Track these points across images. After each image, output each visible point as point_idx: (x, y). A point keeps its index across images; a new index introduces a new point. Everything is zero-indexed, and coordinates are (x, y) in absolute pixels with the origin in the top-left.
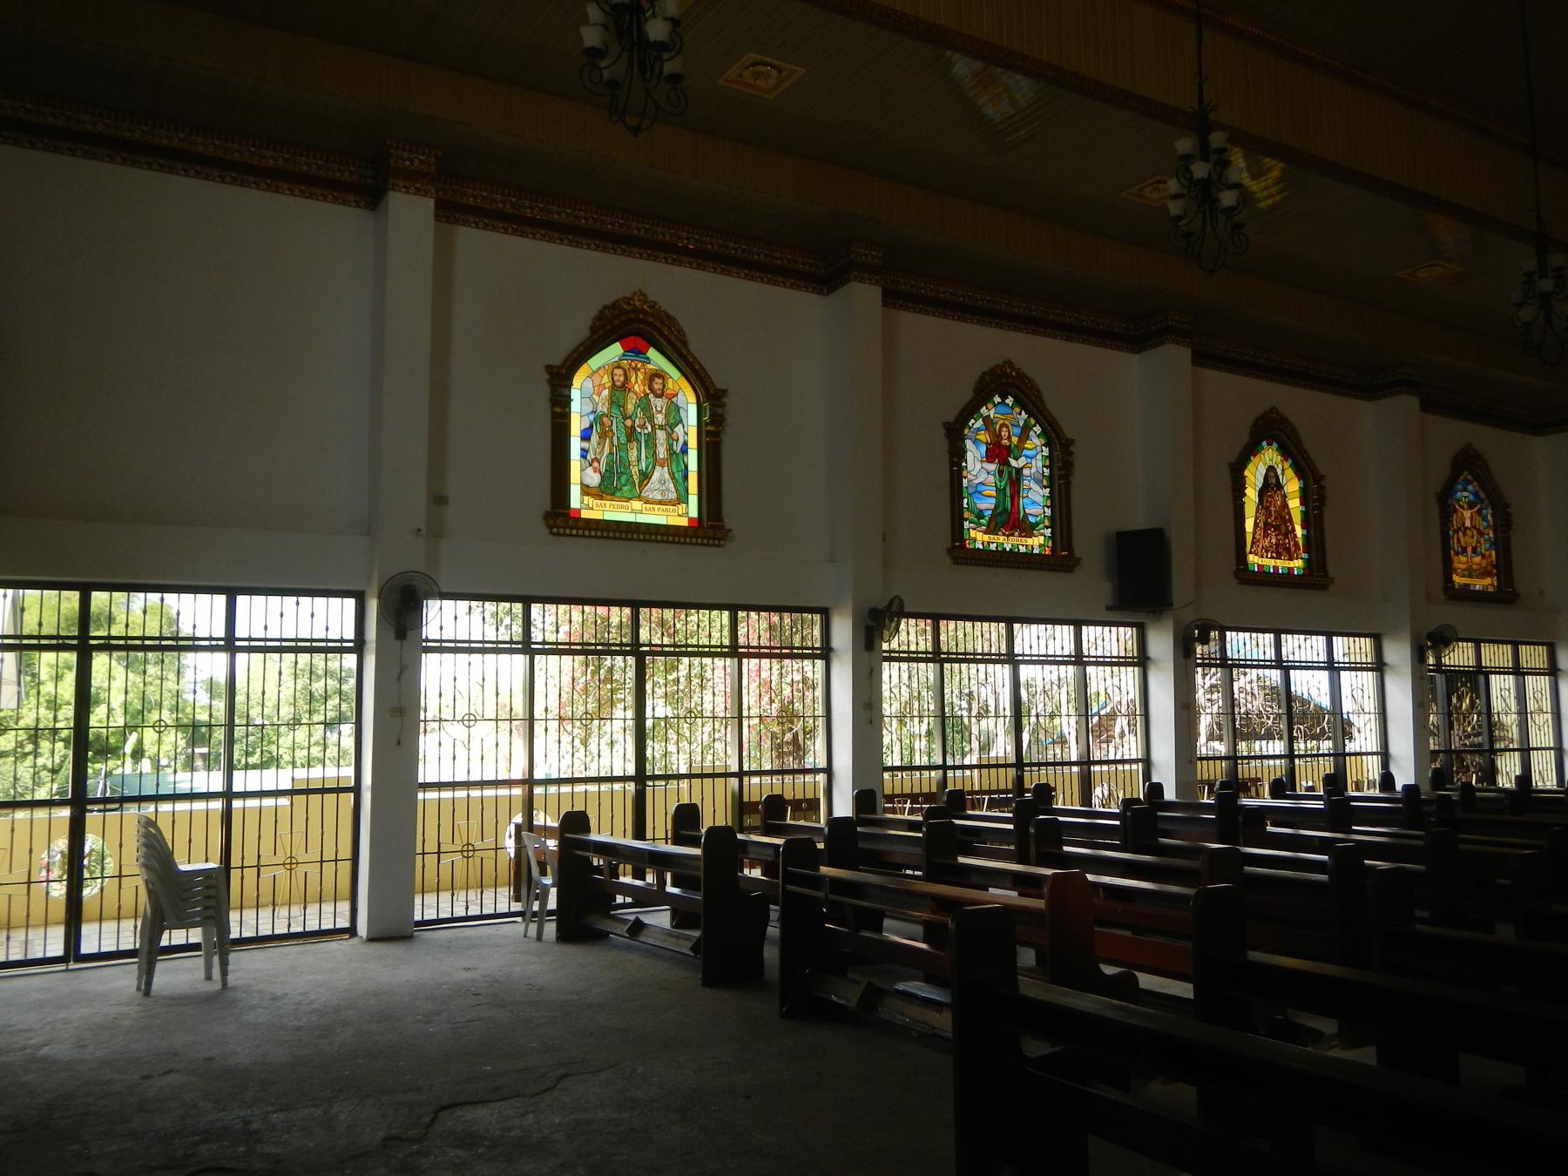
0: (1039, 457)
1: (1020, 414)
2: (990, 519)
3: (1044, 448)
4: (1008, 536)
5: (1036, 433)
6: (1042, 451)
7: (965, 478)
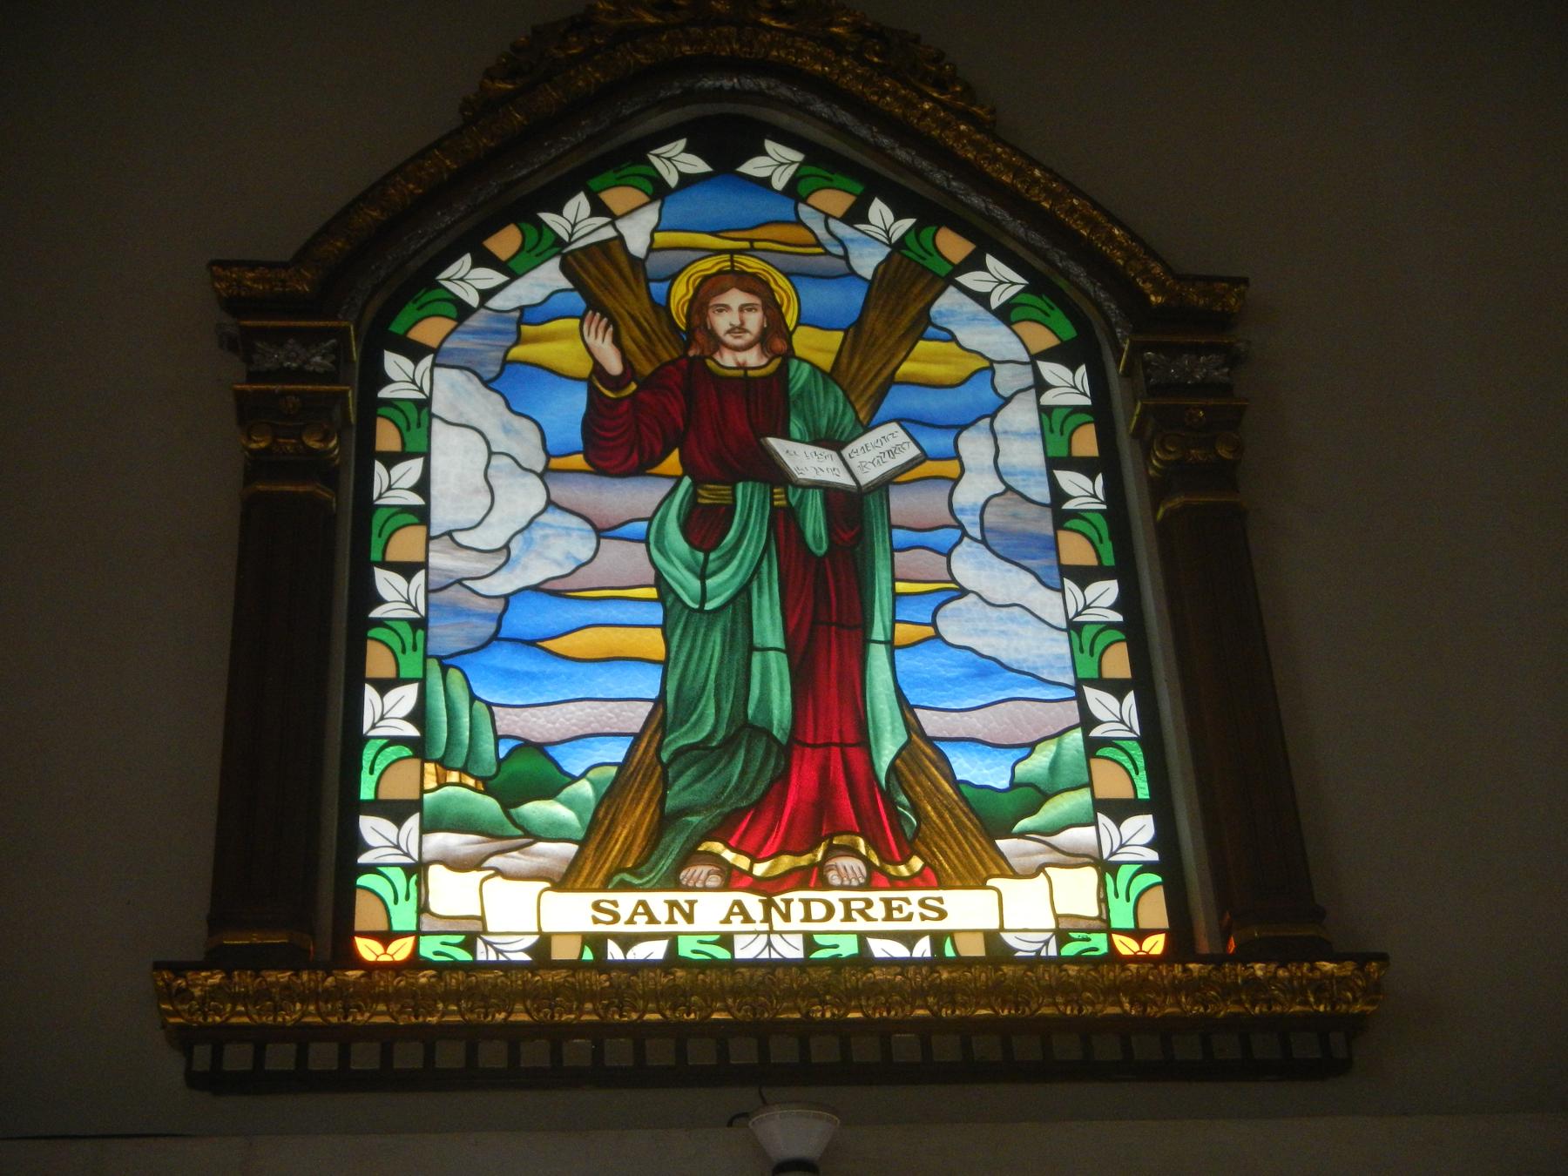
0: (1021, 416)
1: (856, 215)
2: (612, 797)
3: (1051, 371)
4: (767, 888)
5: (982, 299)
6: (1041, 386)
7: (406, 570)
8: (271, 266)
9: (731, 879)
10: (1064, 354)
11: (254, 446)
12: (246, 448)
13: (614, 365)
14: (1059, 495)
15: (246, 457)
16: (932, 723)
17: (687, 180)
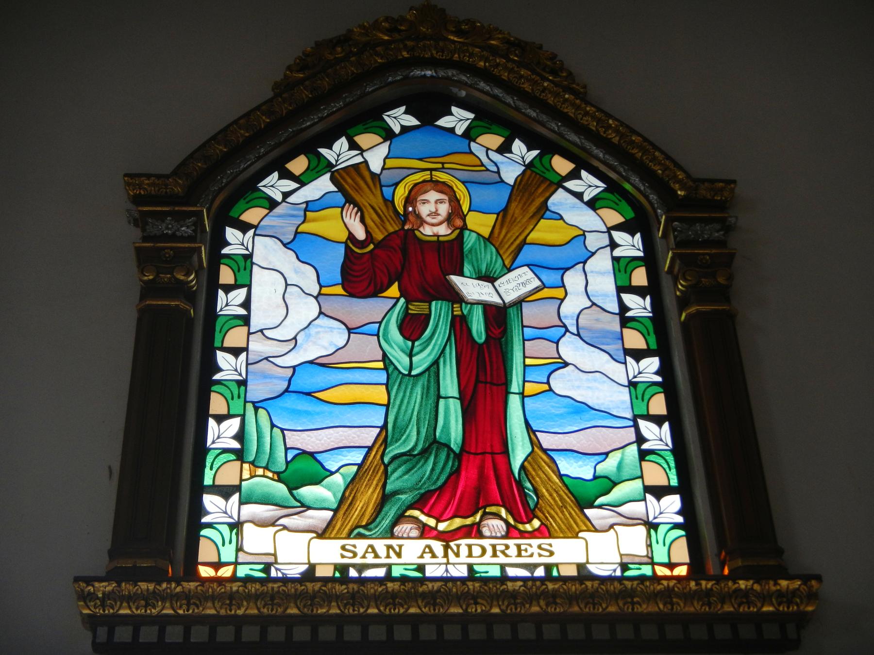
0: (602, 263)
2: (353, 482)
4: (446, 538)
5: (579, 196)
6: (613, 245)
7: (236, 352)
8: (158, 176)
9: (425, 532)
10: (625, 227)
11: (146, 278)
12: (141, 280)
13: (361, 235)
14: (623, 308)
15: (141, 285)
16: (547, 441)
17: (405, 129)
